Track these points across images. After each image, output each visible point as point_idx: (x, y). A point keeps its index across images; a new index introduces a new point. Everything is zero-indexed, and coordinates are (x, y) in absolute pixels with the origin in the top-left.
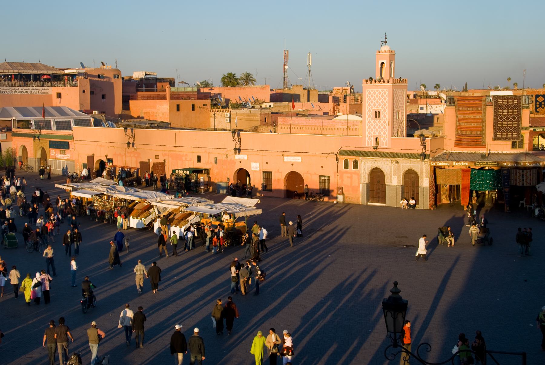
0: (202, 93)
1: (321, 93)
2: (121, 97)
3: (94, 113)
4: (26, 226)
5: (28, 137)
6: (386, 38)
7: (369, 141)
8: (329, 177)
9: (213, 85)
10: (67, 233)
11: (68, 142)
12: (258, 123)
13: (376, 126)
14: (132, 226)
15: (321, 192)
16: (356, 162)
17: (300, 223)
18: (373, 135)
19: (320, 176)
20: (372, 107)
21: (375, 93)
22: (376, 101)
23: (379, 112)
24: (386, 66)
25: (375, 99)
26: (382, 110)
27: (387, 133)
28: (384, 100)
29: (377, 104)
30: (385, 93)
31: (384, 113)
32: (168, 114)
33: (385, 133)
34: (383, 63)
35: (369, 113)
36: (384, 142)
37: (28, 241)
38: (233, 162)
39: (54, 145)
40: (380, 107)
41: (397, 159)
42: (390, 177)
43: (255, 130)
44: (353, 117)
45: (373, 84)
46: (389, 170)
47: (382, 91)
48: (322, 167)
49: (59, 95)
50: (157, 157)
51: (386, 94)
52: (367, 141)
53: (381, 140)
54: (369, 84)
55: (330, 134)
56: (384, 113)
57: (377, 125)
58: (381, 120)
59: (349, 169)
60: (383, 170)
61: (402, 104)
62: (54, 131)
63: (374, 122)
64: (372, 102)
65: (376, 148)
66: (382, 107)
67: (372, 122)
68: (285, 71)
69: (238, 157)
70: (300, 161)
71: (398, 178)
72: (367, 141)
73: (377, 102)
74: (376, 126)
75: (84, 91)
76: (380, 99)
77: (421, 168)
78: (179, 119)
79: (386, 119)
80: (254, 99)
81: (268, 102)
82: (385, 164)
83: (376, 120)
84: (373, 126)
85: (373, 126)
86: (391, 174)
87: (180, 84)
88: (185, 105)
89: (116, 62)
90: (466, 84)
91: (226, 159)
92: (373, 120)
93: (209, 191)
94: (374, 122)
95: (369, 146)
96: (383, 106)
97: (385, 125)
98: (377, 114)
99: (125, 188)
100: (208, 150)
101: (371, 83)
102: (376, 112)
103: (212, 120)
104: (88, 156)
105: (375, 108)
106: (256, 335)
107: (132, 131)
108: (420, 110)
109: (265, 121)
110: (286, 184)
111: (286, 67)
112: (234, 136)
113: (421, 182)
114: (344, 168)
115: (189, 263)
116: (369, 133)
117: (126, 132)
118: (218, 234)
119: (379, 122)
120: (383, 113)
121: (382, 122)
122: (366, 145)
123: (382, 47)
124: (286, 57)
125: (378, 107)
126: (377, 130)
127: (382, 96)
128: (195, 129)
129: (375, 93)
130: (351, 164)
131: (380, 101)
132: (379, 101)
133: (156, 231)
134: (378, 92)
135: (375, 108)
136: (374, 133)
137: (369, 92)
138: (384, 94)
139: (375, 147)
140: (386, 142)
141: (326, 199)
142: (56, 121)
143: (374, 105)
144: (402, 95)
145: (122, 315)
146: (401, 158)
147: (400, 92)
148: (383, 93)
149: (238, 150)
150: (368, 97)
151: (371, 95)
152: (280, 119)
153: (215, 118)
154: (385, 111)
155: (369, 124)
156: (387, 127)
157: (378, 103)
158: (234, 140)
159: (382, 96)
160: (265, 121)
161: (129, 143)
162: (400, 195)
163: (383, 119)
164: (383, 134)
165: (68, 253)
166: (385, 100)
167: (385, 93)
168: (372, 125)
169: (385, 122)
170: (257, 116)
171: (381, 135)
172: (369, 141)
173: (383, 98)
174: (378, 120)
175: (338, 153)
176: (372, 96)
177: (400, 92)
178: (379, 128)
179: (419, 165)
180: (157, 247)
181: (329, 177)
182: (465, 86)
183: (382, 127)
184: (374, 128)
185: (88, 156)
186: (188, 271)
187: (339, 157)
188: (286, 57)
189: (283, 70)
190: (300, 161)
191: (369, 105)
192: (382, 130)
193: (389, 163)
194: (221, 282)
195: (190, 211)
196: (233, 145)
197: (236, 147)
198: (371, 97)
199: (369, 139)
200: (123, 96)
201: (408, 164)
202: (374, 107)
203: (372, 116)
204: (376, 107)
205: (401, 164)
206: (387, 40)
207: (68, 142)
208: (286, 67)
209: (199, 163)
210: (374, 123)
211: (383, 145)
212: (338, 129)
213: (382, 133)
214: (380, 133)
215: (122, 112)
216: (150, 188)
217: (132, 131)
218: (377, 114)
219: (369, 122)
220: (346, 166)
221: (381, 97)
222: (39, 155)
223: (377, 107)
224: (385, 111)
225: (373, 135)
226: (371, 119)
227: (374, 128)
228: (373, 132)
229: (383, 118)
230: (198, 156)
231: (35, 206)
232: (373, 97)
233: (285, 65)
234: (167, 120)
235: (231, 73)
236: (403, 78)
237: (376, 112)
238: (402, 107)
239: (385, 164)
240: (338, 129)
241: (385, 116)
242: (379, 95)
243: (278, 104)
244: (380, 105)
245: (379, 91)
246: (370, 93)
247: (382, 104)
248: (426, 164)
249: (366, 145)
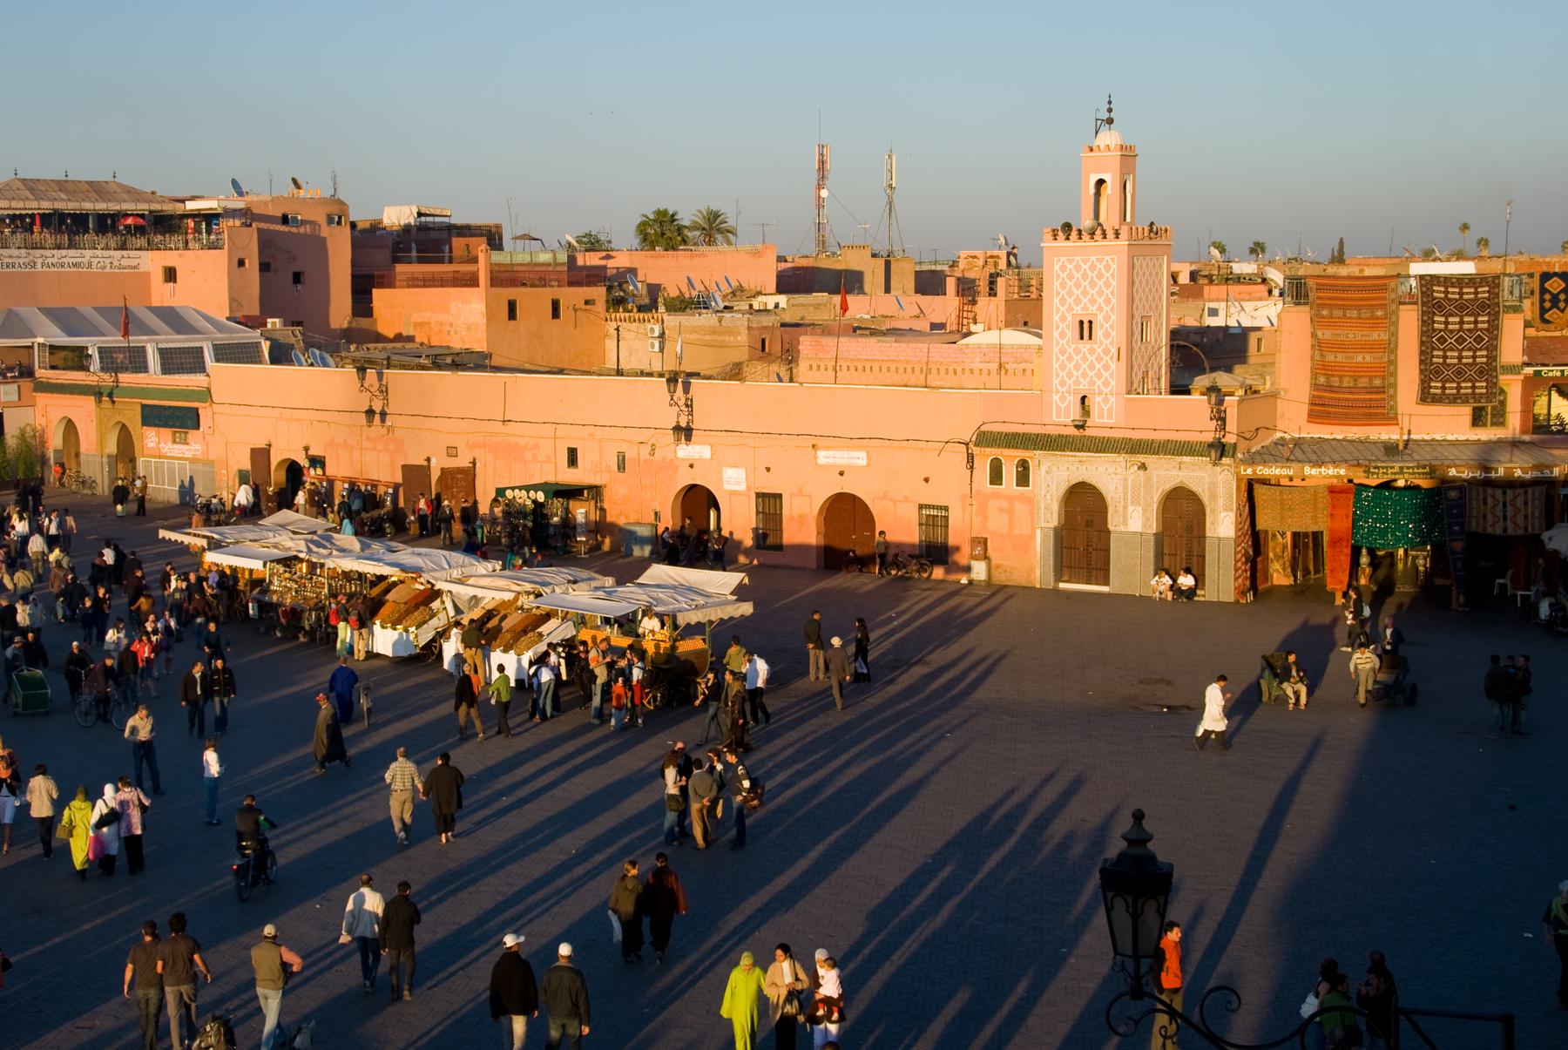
0: (581, 267)
1: (925, 268)
2: (349, 278)
3: (269, 326)
4: (76, 651)
5: (80, 393)
6: (1110, 110)
7: (1062, 406)
8: (946, 509)
9: (613, 246)
10: (194, 671)
11: (197, 409)
12: (741, 355)
13: (1081, 363)
14: (381, 651)
15: (924, 553)
16: (1024, 467)
17: (864, 643)
18: (1073, 387)
19: (921, 507)
20: (1070, 309)
21: (1078, 268)
22: (1080, 290)
23: (1090, 322)
24: (1109, 190)
25: (1078, 285)
26: (1100, 318)
27: (1113, 383)
28: (1103, 289)
29: (1085, 300)
30: (1107, 268)
31: (1106, 325)
32: (484, 328)
33: (1106, 383)
34: (1101, 182)
35: (1061, 326)
36: (1106, 408)
37: (80, 694)
38: (671, 465)
39: (155, 417)
40: (1093, 309)
41: (1142, 458)
42: (1121, 509)
43: (735, 373)
44: (1016, 338)
45: (1074, 243)
46: (1121, 488)
47: (1100, 261)
48: (927, 480)
49: (170, 275)
50: (452, 451)
51: (1111, 272)
52: (1057, 405)
53: (1095, 403)
54: (1061, 242)
55: (949, 386)
56: (1106, 325)
57: (1085, 359)
58: (1095, 346)
59: (1003, 487)
60: (1103, 490)
61: (1157, 298)
62: (154, 376)
63: (1077, 351)
64: (1070, 294)
65: (1081, 427)
66: (1100, 309)
67: (1071, 350)
68: (820, 203)
69: (685, 451)
70: (863, 462)
71: (1145, 511)
72: (1057, 405)
73: (1085, 293)
74: (1081, 363)
75: (241, 263)
76: (1093, 284)
77: (1212, 483)
78: (514, 343)
79: (1112, 343)
80: (730, 286)
81: (771, 294)
82: (1107, 473)
83: (1081, 346)
84: (1074, 362)
85: (1074, 362)
86: (1125, 499)
87: (518, 241)
88: (534, 301)
89: (334, 178)
90: (1341, 243)
91: (652, 458)
92: (1074, 346)
93: (600, 549)
94: (1077, 351)
95: (1063, 420)
96: (1103, 305)
97: (1108, 358)
98: (1085, 329)
99: (360, 541)
100: (599, 432)
101: (1068, 239)
102: (1081, 323)
103: (611, 344)
104: (252, 449)
105: (1080, 312)
106: (737, 964)
107: (380, 376)
108: (1209, 315)
109: (762, 349)
110: (823, 530)
111: (824, 193)
112: (672, 392)
113: (1212, 523)
114: (991, 483)
115: (544, 756)
116: (1063, 383)
117: (364, 379)
118: (627, 672)
119: (1092, 351)
120: (1102, 326)
121: (1100, 350)
122: (1054, 419)
123: (1099, 135)
124: (822, 163)
125: (1087, 309)
126: (1085, 375)
127: (1100, 276)
128: (561, 372)
129: (1078, 268)
130: (1010, 472)
131: (1094, 291)
132: (1091, 292)
133: (450, 663)
134: (1088, 264)
135: (1078, 310)
136: (1077, 383)
137: (1060, 264)
138: (1103, 271)
139: (1078, 423)
140: (1111, 407)
141: (938, 573)
142: (162, 349)
143: (1077, 301)
144: (1157, 273)
145: (350, 906)
146: (1153, 454)
147: (1151, 265)
148: (1102, 266)
149: (685, 432)
150: (1058, 279)
151: (1066, 273)
152: (806, 344)
153: (618, 341)
154: (1107, 318)
155: (1061, 358)
156: (1113, 366)
157: (1089, 297)
158: (673, 403)
159: (1100, 276)
160: (762, 349)
161: (370, 413)
162: (1152, 560)
163: (1101, 344)
164: (1101, 387)
165: (196, 728)
166: (1108, 288)
167: (1107, 268)
168: (1070, 359)
169: (1106, 352)
170: (739, 333)
171: (1096, 387)
172: (1062, 406)
173: (1101, 283)
174: (1088, 346)
175: (974, 439)
176: (1070, 277)
177: (1151, 265)
178: (1092, 367)
179: (1205, 475)
180: (452, 710)
181: (946, 509)
182: (1336, 248)
183: (1098, 366)
184: (1077, 367)
185: (252, 449)
186: (540, 779)
187: (976, 450)
188: (822, 163)
189: (813, 202)
190: (863, 462)
191: (1063, 301)
192: (1099, 375)
193: (1120, 470)
194: (635, 812)
195: (546, 608)
196: (670, 417)
197: (678, 422)
198: (1066, 280)
199: (1063, 399)
200: (353, 277)
201: (1175, 473)
202: (1076, 308)
203: (1069, 334)
204: (1083, 309)
205: (1155, 473)
206: (1112, 115)
207: (197, 409)
208: (824, 193)
209: (572, 470)
210: (1077, 355)
211: (1101, 416)
212: (972, 371)
213: (1099, 383)
214: (1092, 383)
215: (350, 322)
216: (433, 540)
217: (380, 376)
218: (1085, 329)
219: (1063, 352)
220: (996, 477)
221: (1096, 280)
222: (112, 447)
223: (1085, 308)
224: (1107, 318)
225: (1073, 387)
226: (1068, 343)
227: (1077, 367)
228: (1073, 379)
229: (1103, 339)
230: (569, 449)
231: (101, 592)
232: (1074, 280)
233: (820, 187)
234: (481, 347)
235: (666, 210)
236: (1158, 225)
237: (1081, 323)
238: (1157, 307)
239: (1107, 473)
240: (972, 371)
241: (1107, 335)
242: (1090, 274)
243: (800, 299)
244: (1093, 301)
245: (1090, 262)
246: (1063, 268)
247: (1100, 300)
248: (1226, 472)
249: (1054, 419)
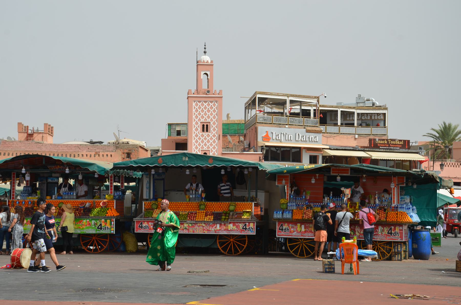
13: (204, 140)
20: (199, 120)
23: (207, 125)
26: (211, 123)
35: (196, 126)
40: (208, 120)
58: (210, 134)
63: (202, 136)
66: (212, 120)
73: (205, 114)
83: (204, 134)
102: (203, 125)
105: (203, 121)
126: (205, 145)
135: (203, 120)
136: (203, 147)
143: (202, 117)
163: (212, 133)
167: (214, 105)
169: (214, 136)
183: (211, 141)
191: (197, 117)
213: (211, 147)
214: (208, 147)
218: (205, 128)
224: (214, 123)
225: (201, 149)
227: (202, 142)
241: (214, 130)
244: (209, 117)
246: (197, 105)
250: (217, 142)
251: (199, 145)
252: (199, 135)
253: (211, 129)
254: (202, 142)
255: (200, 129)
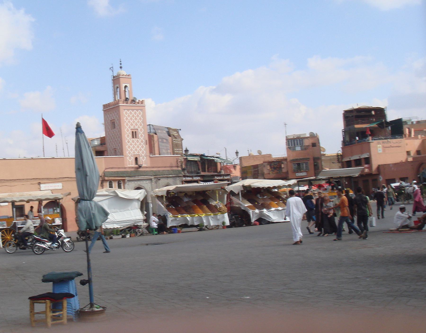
20: (130, 127)
23: (136, 132)
26: (139, 130)
63: (133, 141)
73: (134, 122)
76: (136, 119)
83: (134, 139)
94: (133, 141)
102: (133, 132)
116: (129, 153)
119: (138, 141)
126: (136, 150)
136: (134, 152)
143: (132, 124)
159: (138, 116)
167: (140, 113)
169: (142, 142)
199: (130, 158)
218: (134, 134)
224: (141, 130)
226: (130, 138)
227: (134, 147)
241: (142, 136)
250: (145, 147)
251: (131, 150)
252: (131, 141)
253: (139, 135)
254: (134, 147)
255: (131, 136)
